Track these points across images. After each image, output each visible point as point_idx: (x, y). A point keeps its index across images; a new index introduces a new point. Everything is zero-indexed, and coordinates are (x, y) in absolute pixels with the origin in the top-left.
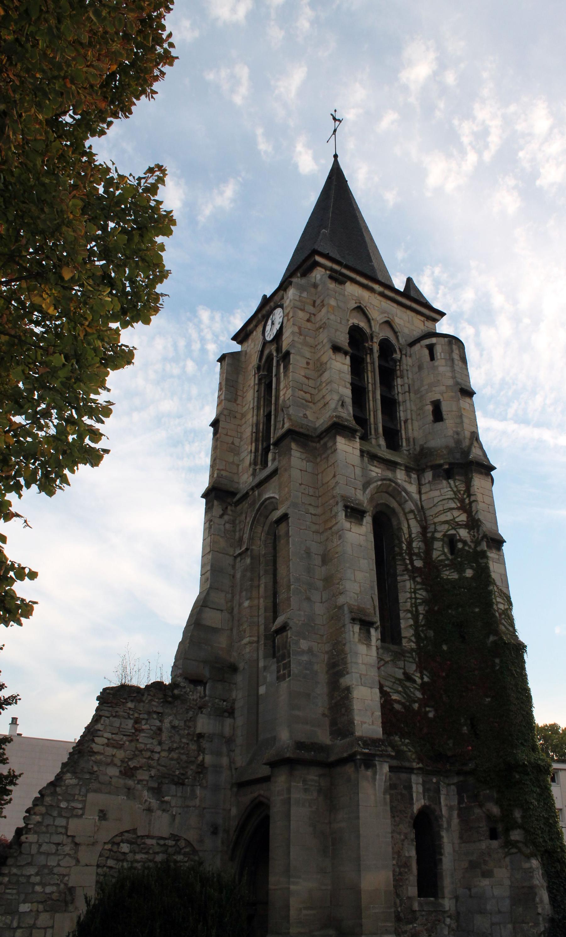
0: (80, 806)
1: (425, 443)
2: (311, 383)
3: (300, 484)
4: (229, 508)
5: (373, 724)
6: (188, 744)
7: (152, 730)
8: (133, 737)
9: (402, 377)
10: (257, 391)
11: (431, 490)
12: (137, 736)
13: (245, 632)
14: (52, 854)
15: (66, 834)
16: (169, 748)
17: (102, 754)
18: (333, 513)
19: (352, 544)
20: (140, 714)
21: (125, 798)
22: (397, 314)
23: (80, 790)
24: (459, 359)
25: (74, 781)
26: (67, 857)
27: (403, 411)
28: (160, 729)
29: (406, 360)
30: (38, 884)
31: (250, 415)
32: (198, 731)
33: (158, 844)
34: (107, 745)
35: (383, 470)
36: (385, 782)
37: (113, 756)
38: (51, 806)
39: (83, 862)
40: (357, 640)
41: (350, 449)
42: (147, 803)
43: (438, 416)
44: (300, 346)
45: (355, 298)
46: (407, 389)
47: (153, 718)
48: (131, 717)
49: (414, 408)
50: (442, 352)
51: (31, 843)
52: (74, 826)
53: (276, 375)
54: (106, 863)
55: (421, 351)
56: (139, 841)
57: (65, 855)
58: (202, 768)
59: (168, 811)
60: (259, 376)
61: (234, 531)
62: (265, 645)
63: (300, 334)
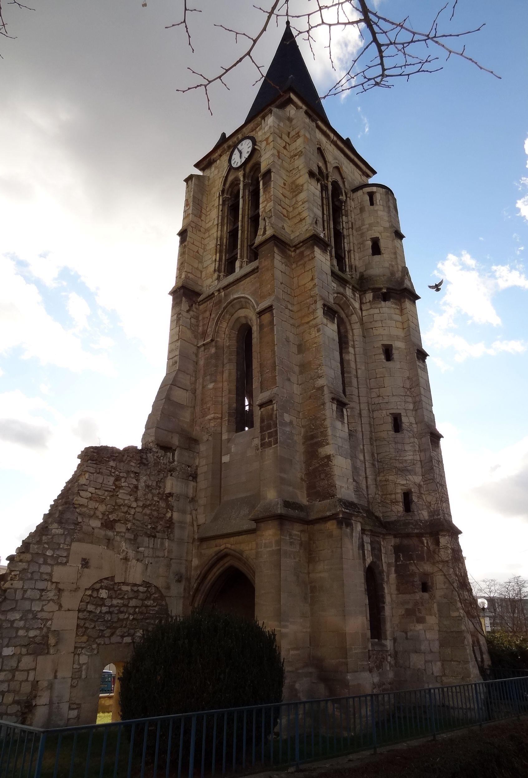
0: (65, 554)
1: (365, 271)
2: (287, 201)
3: (281, 283)
4: (194, 305)
6: (158, 502)
7: (130, 488)
8: (113, 493)
9: (347, 216)
10: (221, 211)
11: (371, 308)
12: (117, 492)
13: (209, 409)
16: (143, 504)
17: (87, 507)
18: (311, 310)
19: (328, 337)
20: (120, 472)
21: (106, 547)
23: (65, 540)
24: (393, 207)
25: (60, 531)
26: (51, 602)
27: (347, 244)
28: (136, 487)
30: (22, 628)
31: (214, 230)
32: (168, 491)
33: (132, 590)
34: (90, 499)
35: (337, 286)
36: (359, 539)
37: (96, 509)
38: (37, 554)
41: (323, 259)
42: (125, 552)
43: (376, 249)
46: (350, 226)
47: (131, 477)
48: (113, 474)
49: (355, 242)
50: (380, 200)
51: (16, 590)
52: (59, 573)
53: (242, 197)
54: (87, 607)
55: (362, 196)
56: (116, 588)
57: (49, 601)
58: (170, 524)
59: (142, 561)
60: (223, 198)
61: (198, 326)
62: (229, 421)
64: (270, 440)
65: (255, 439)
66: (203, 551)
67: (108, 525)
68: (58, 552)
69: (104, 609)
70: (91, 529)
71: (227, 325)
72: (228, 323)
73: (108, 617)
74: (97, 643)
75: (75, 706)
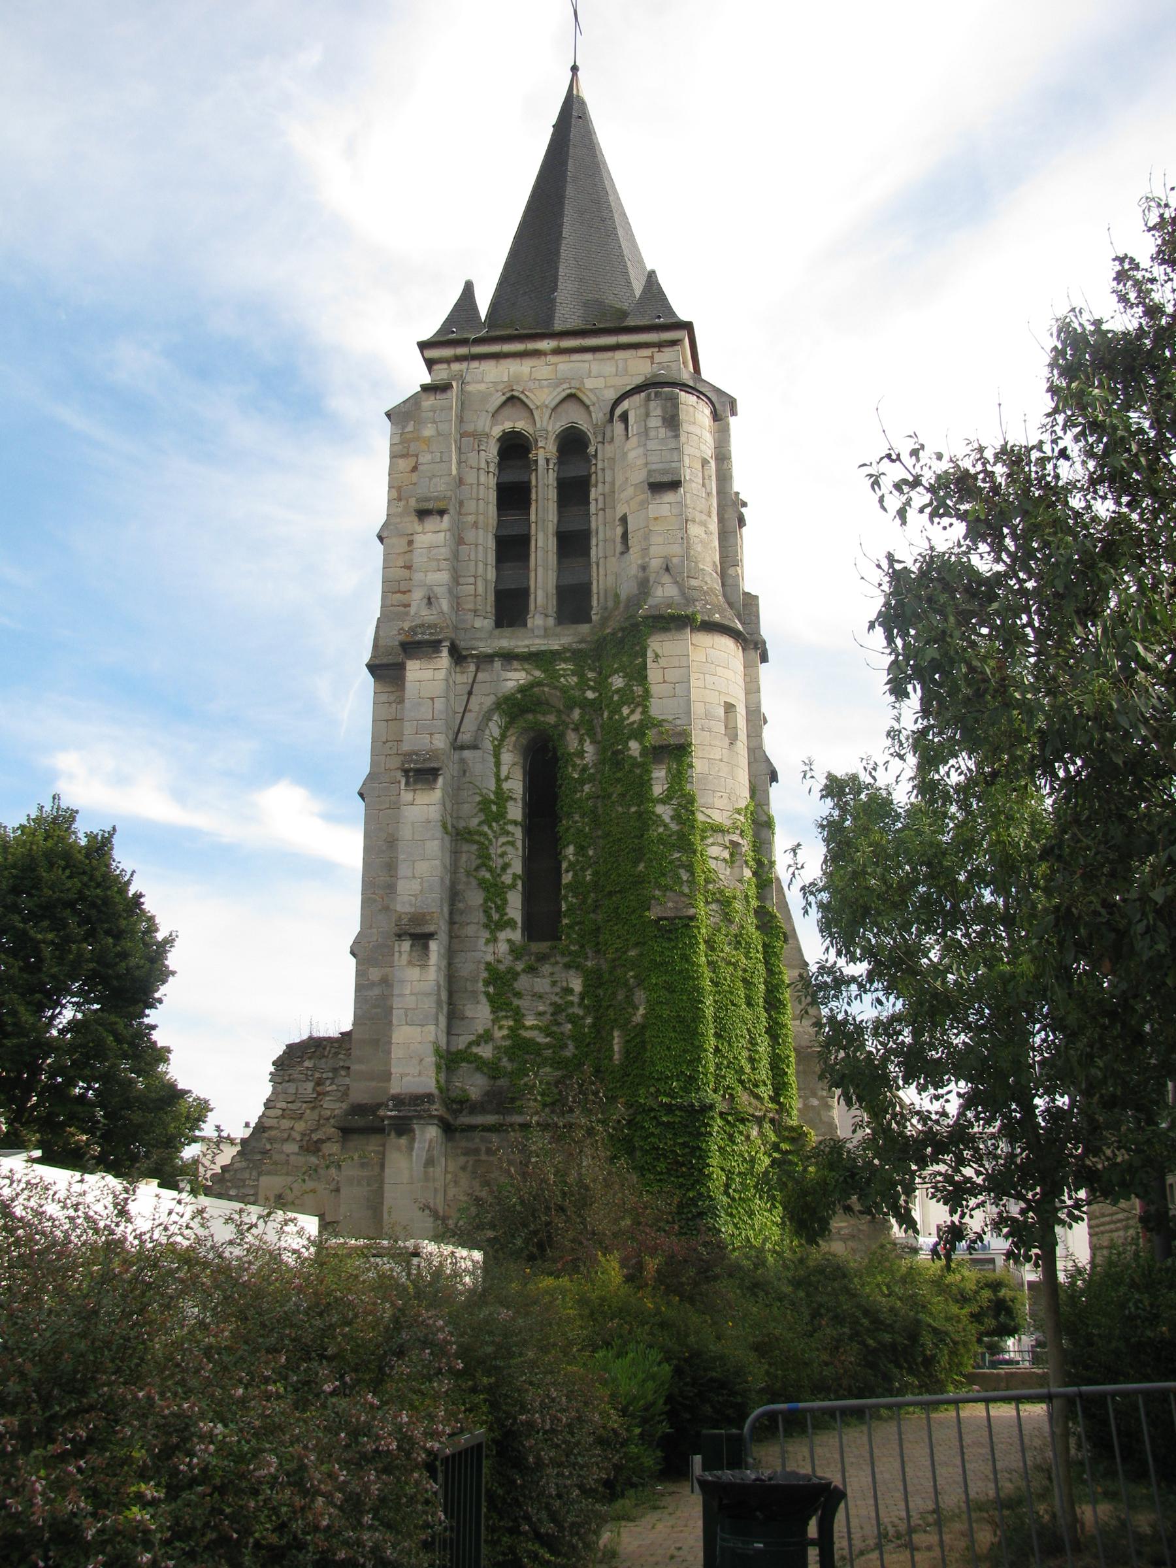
5: (420, 1074)
17: (277, 1128)
19: (413, 823)
22: (590, 372)
24: (660, 424)
25: (244, 1164)
29: (603, 450)
34: (283, 1116)
37: (292, 1128)
40: (404, 962)
41: (427, 674)
44: (398, 520)
45: (500, 387)
63: (400, 499)
68: (243, 1191)
70: (283, 1157)
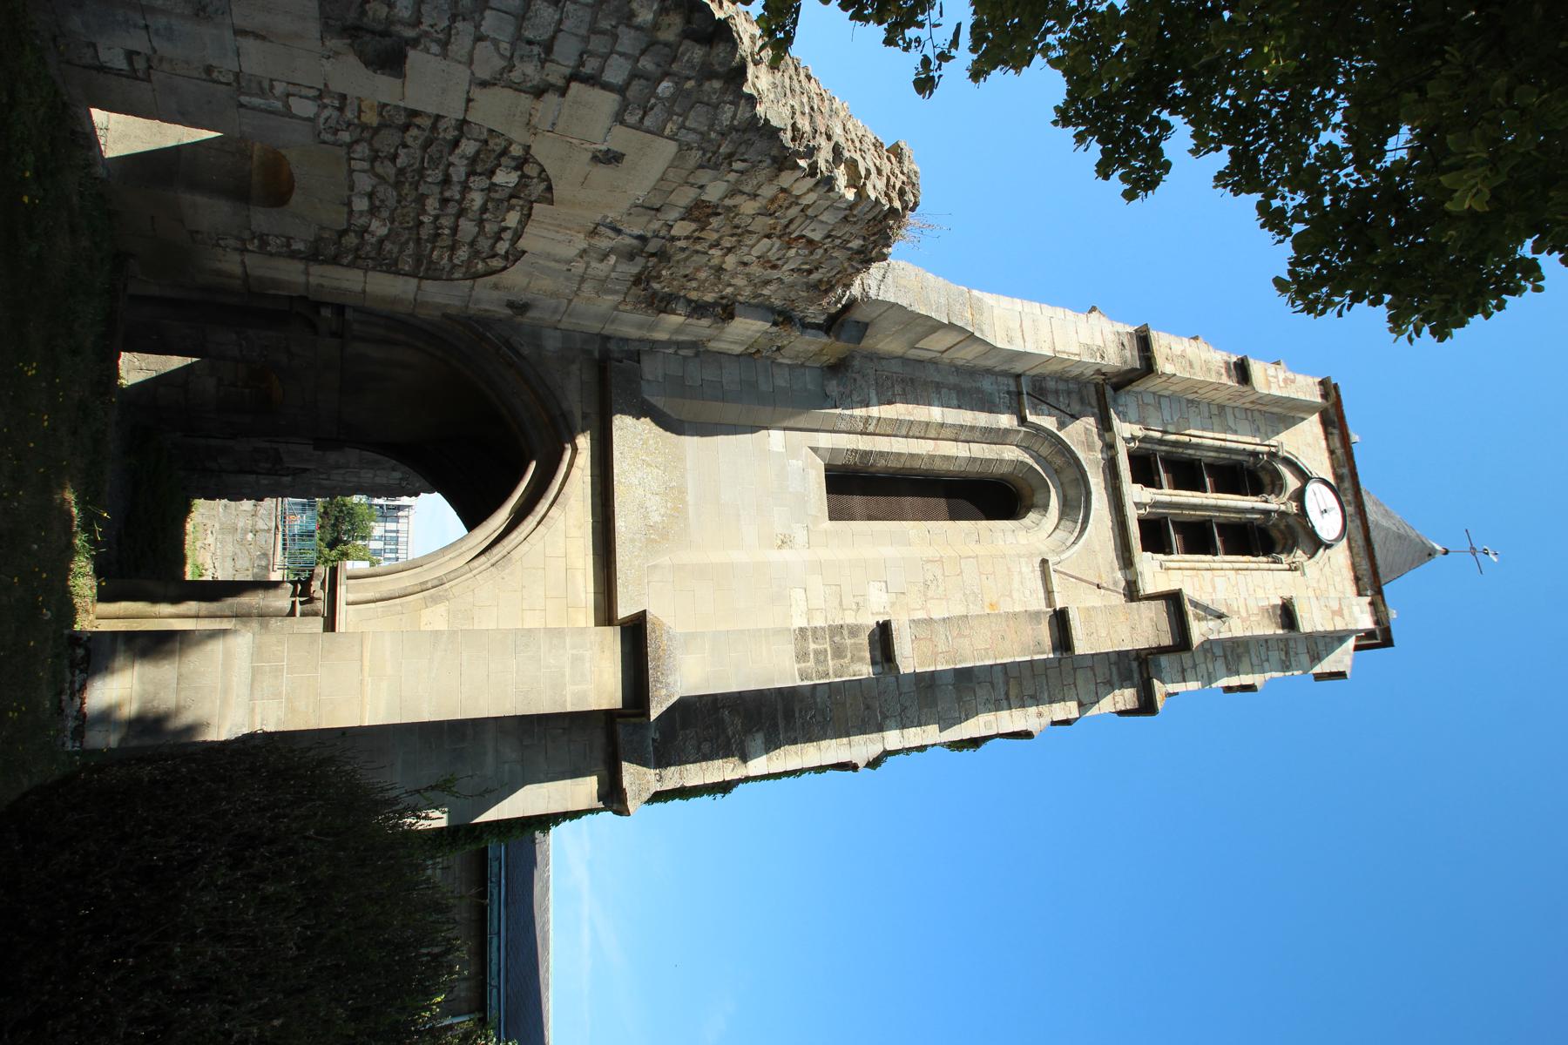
14: (519, 28)
15: (574, 77)
39: (476, 93)
64: (812, 656)
65: (805, 532)
66: (575, 368)
67: (700, 212)
69: (458, 172)
71: (1040, 456)
72: (1045, 458)
73: (434, 175)
74: (356, 142)
75: (140, 64)
